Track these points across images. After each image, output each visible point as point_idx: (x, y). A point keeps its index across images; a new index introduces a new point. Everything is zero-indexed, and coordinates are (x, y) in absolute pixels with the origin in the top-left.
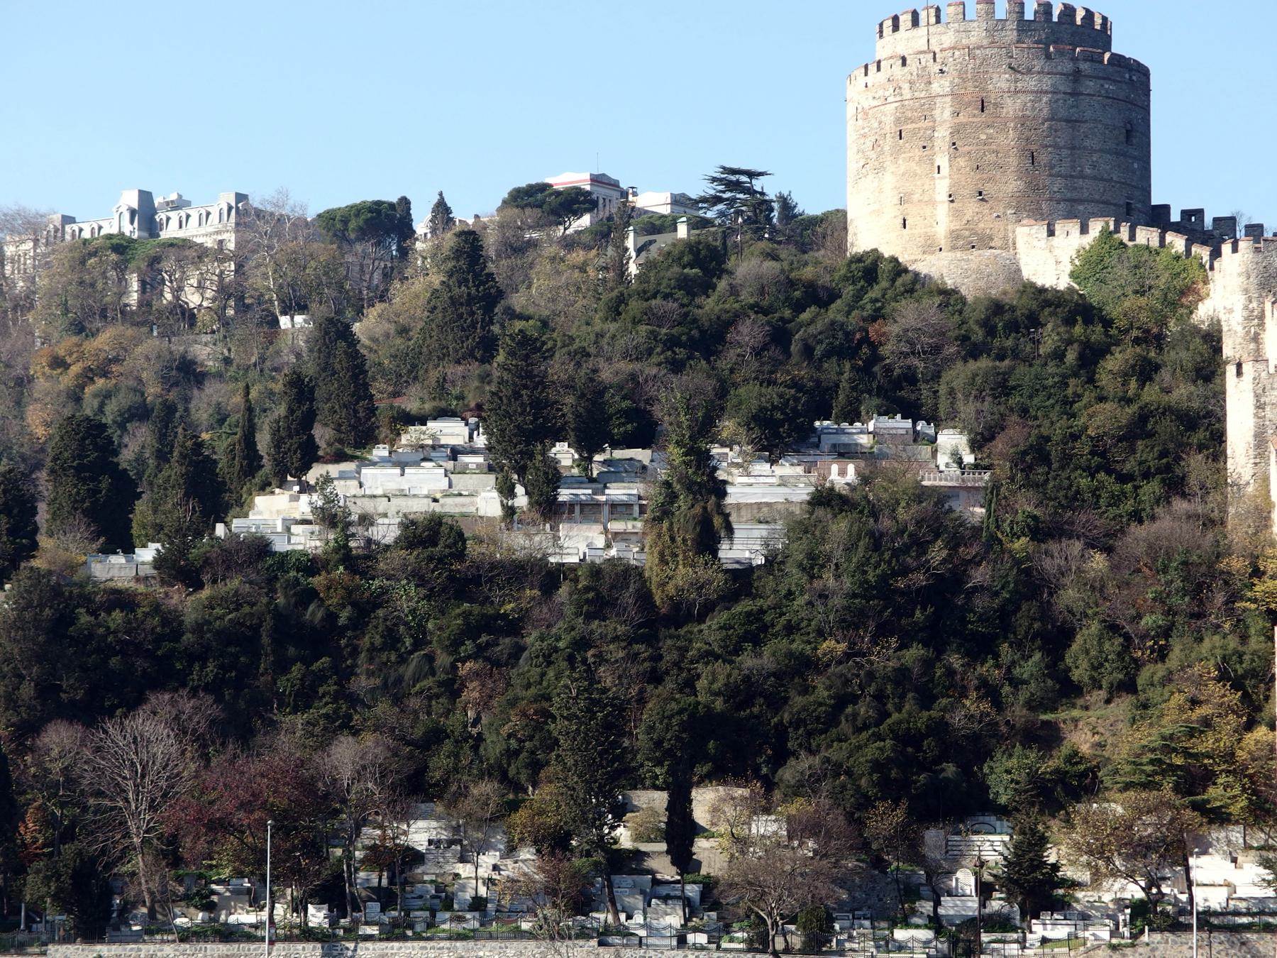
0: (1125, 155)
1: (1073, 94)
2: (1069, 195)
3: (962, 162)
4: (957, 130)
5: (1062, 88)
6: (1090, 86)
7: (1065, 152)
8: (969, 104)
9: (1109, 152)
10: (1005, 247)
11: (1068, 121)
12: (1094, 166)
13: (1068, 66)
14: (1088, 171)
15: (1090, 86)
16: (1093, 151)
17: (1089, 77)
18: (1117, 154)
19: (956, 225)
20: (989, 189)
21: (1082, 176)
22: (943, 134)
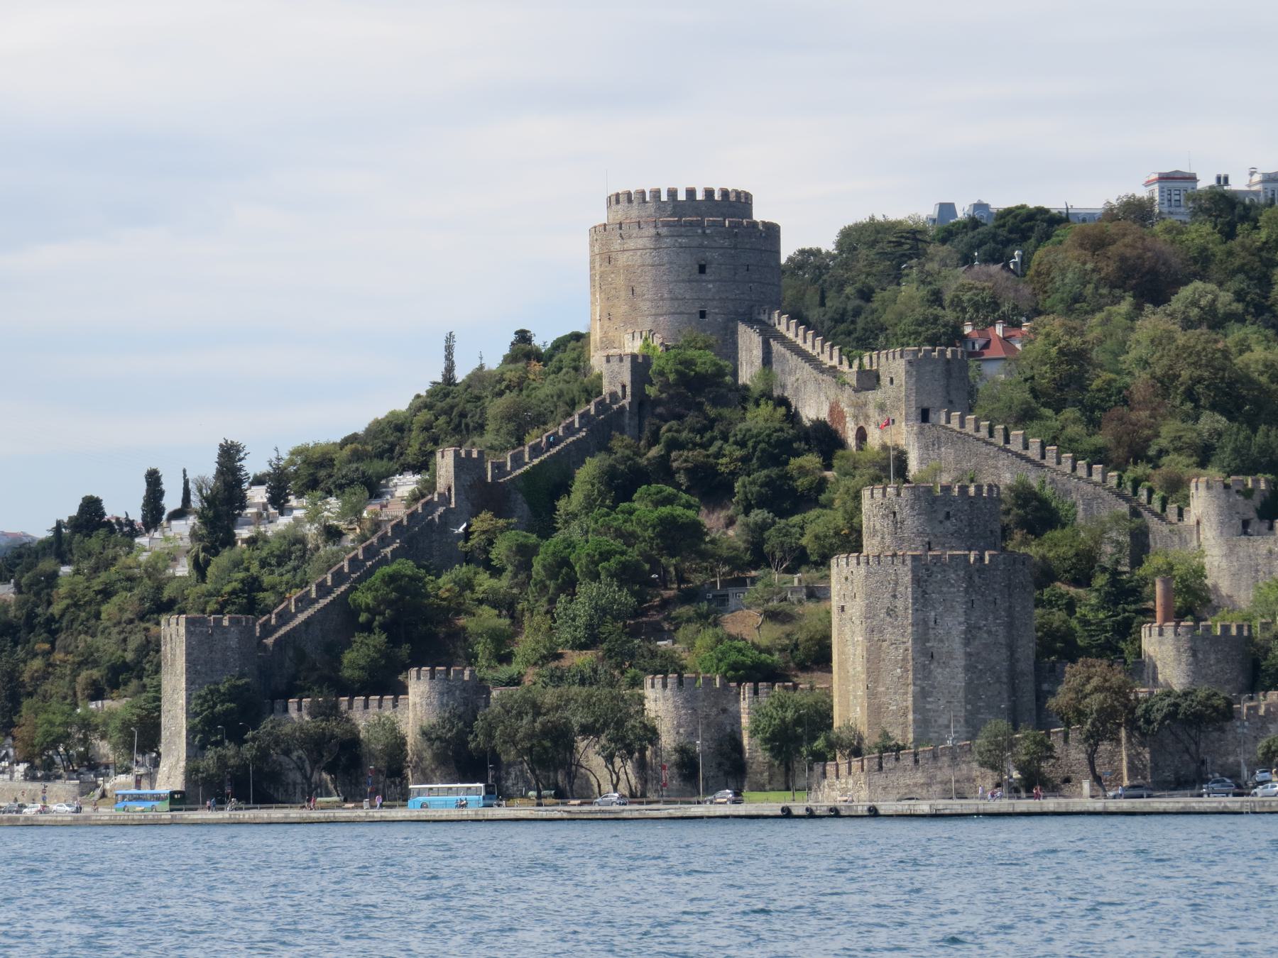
1: (655, 249)
5: (648, 245)
9: (683, 281)
10: (620, 348)
13: (652, 231)
17: (667, 236)
18: (690, 281)
20: (613, 311)
22: (597, 278)
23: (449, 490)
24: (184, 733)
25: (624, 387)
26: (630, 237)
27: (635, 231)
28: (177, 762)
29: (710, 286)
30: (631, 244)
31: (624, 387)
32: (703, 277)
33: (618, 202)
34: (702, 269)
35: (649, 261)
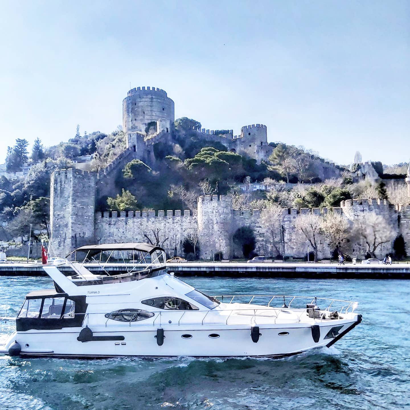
0: (162, 112)
1: (151, 101)
2: (150, 119)
3: (133, 114)
4: (132, 109)
6: (155, 100)
7: (150, 111)
8: (134, 104)
9: (159, 111)
11: (150, 106)
12: (155, 114)
13: (151, 97)
14: (154, 115)
15: (155, 100)
16: (155, 111)
17: (155, 99)
18: (161, 112)
19: (132, 125)
20: (137, 118)
21: (153, 115)
23: (134, 147)
24: (70, 225)
25: (167, 129)
26: (143, 98)
27: (145, 97)
28: (65, 239)
29: (165, 114)
30: (144, 100)
31: (167, 129)
32: (164, 111)
33: (130, 93)
34: (163, 109)
35: (149, 105)
